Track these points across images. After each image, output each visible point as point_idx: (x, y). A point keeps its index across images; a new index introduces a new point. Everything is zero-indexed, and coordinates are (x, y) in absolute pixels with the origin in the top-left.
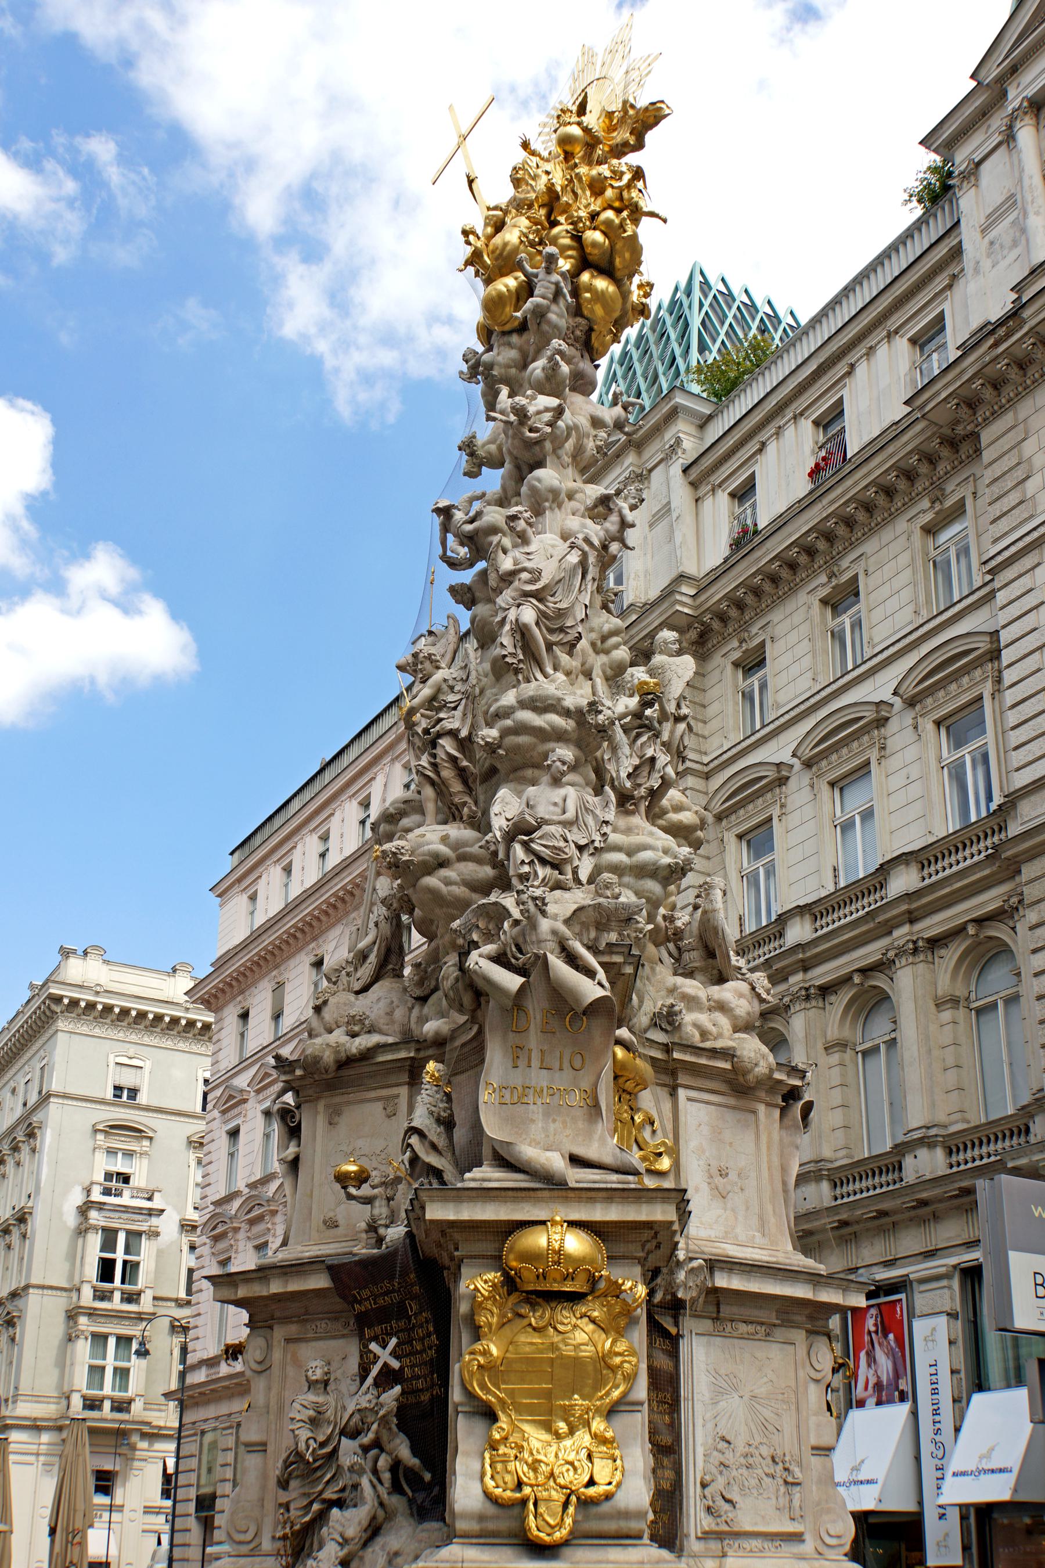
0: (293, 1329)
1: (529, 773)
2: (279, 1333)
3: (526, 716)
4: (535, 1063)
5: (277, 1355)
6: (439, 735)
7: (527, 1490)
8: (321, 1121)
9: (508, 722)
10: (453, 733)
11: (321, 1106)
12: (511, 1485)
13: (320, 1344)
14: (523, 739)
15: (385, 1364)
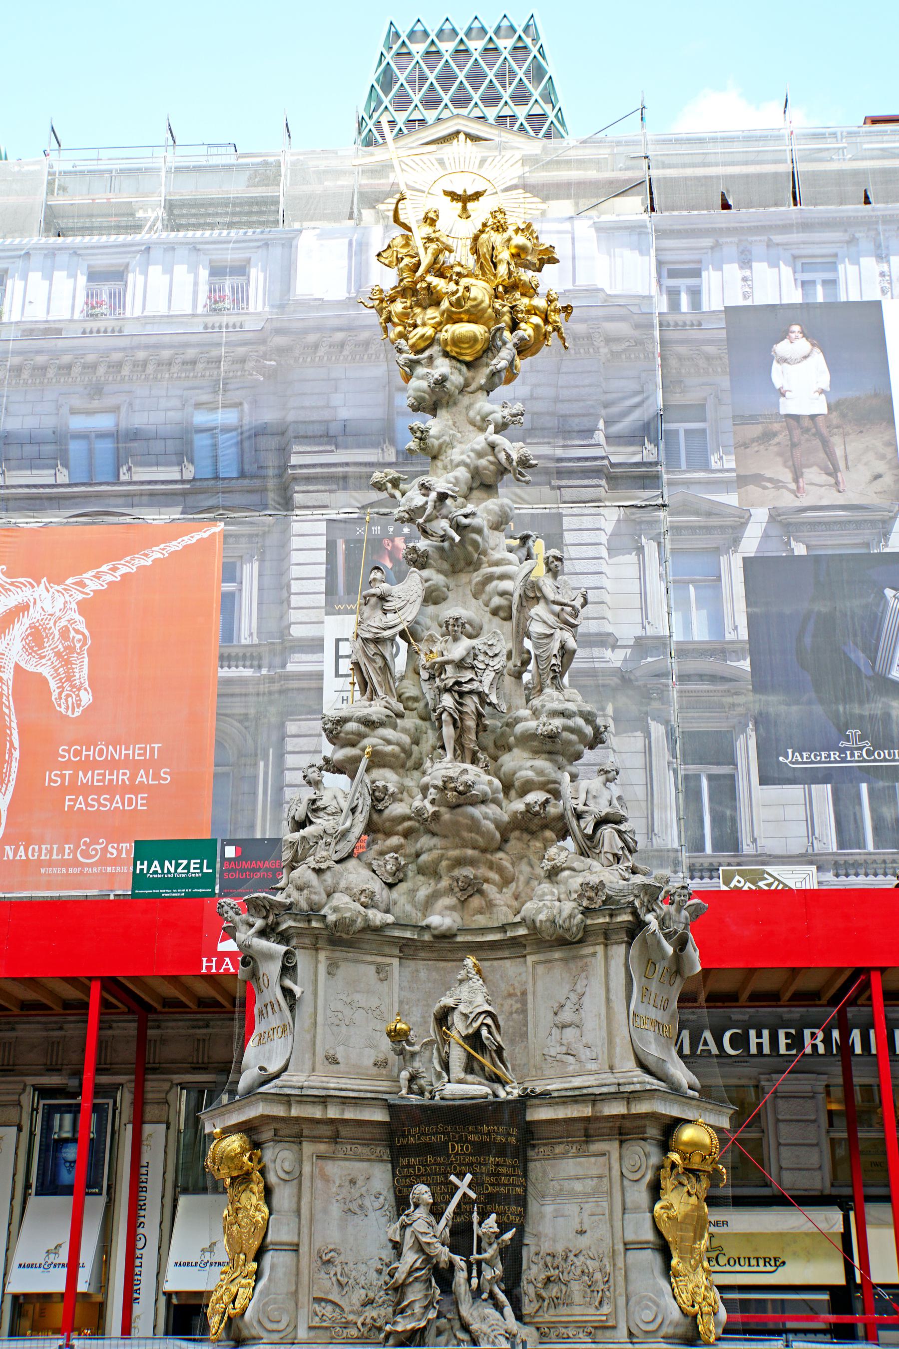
0: (322, 1148)
1: (560, 758)
2: (308, 1148)
3: (580, 722)
4: (652, 1002)
5: (307, 1169)
6: (471, 692)
7: (697, 1307)
8: (322, 968)
9: (570, 723)
10: (481, 695)
11: (322, 955)
12: (690, 1303)
13: (347, 1163)
14: (574, 737)
15: (465, 1194)
